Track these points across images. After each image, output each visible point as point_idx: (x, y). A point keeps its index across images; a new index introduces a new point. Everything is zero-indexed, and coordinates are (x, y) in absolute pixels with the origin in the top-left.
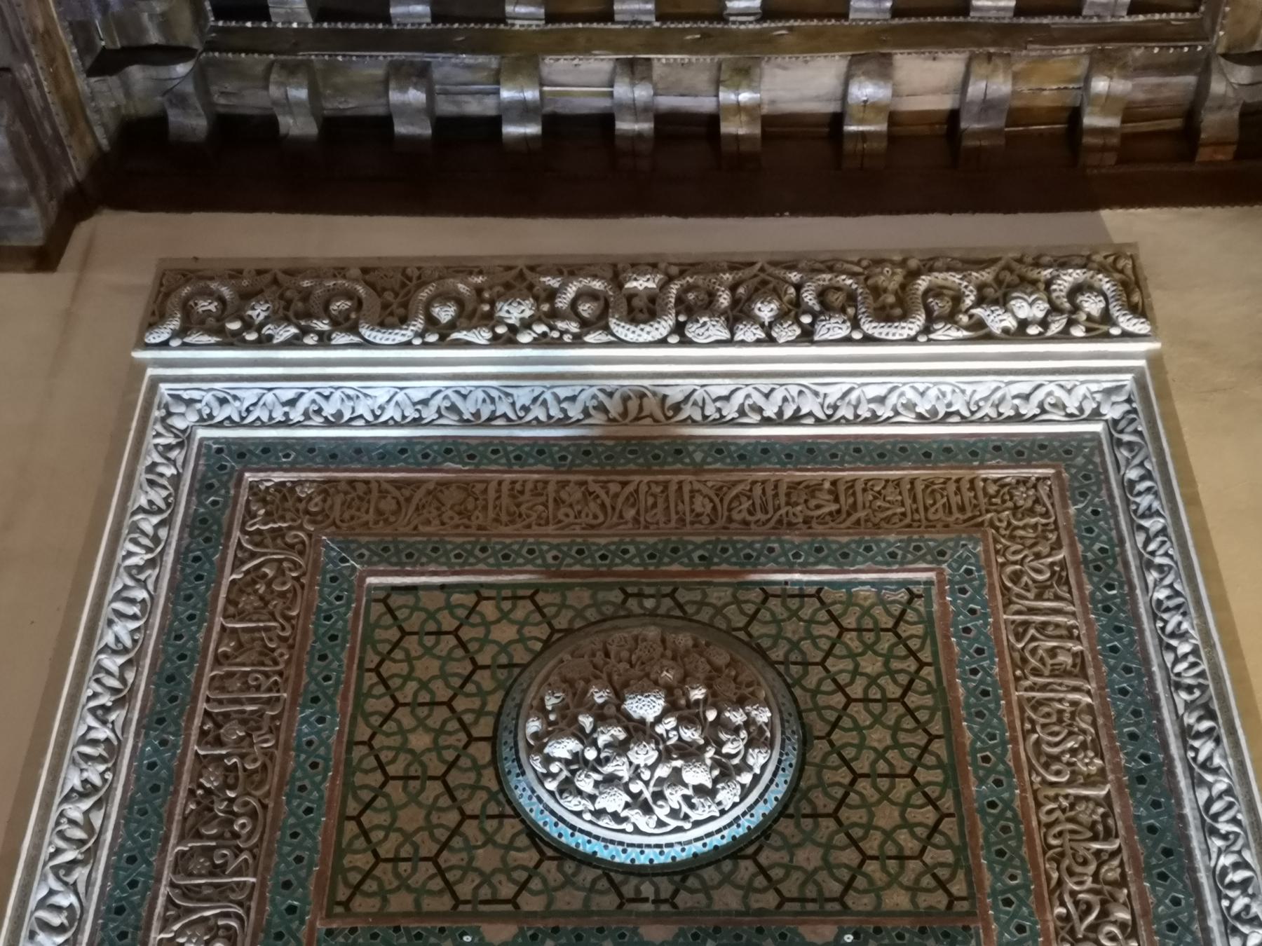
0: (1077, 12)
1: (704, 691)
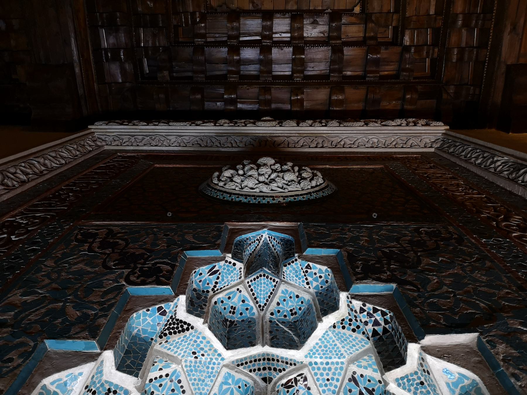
1: (292, 164)
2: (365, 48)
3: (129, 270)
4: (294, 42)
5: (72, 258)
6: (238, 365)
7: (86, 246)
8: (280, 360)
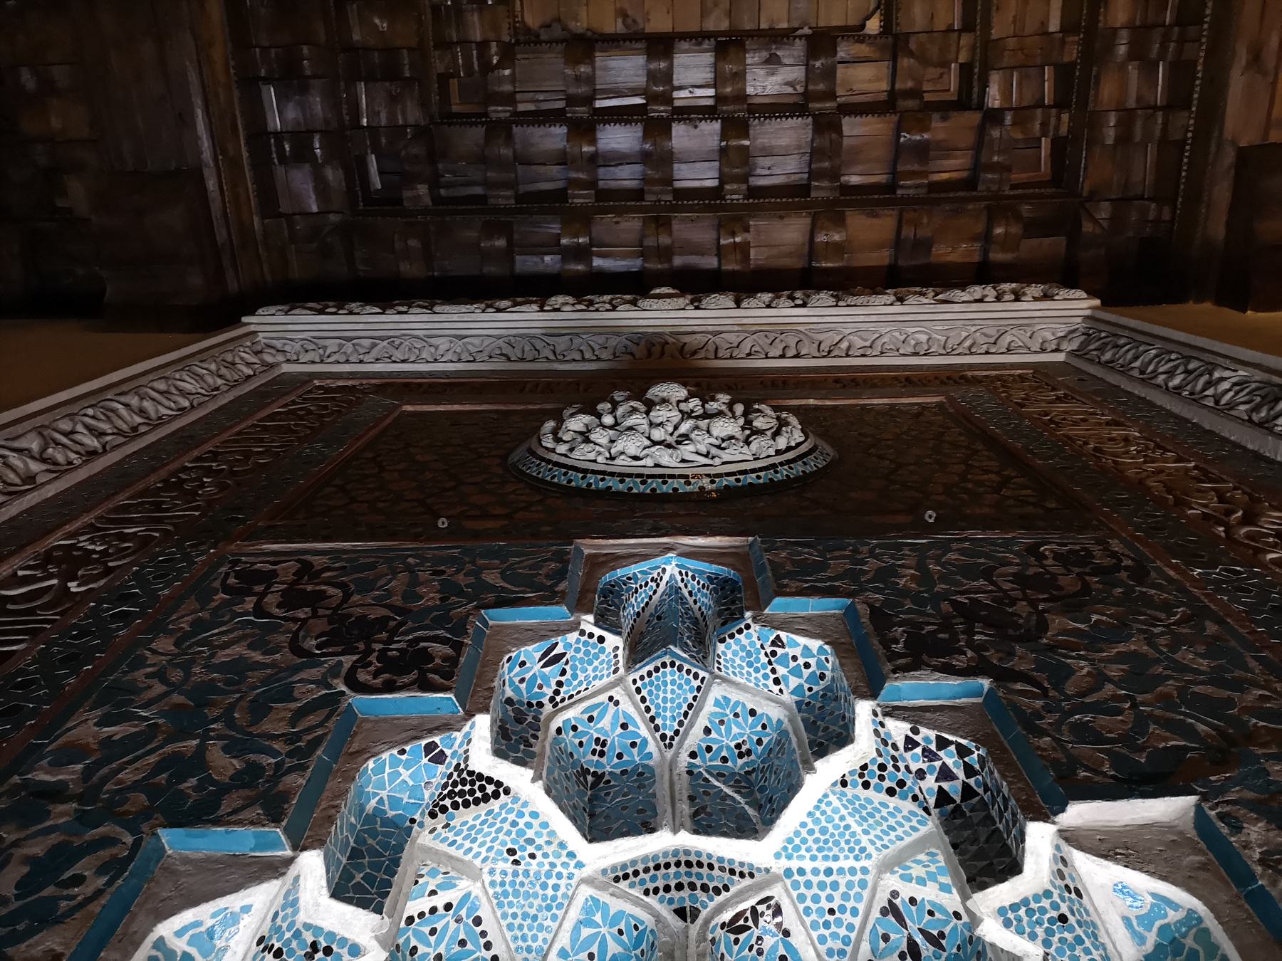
0: (975, 189)
1: (729, 397)
2: (895, 118)
3: (355, 657)
4: (724, 108)
5: (216, 631)
6: (617, 879)
7: (249, 603)
8: (716, 866)
